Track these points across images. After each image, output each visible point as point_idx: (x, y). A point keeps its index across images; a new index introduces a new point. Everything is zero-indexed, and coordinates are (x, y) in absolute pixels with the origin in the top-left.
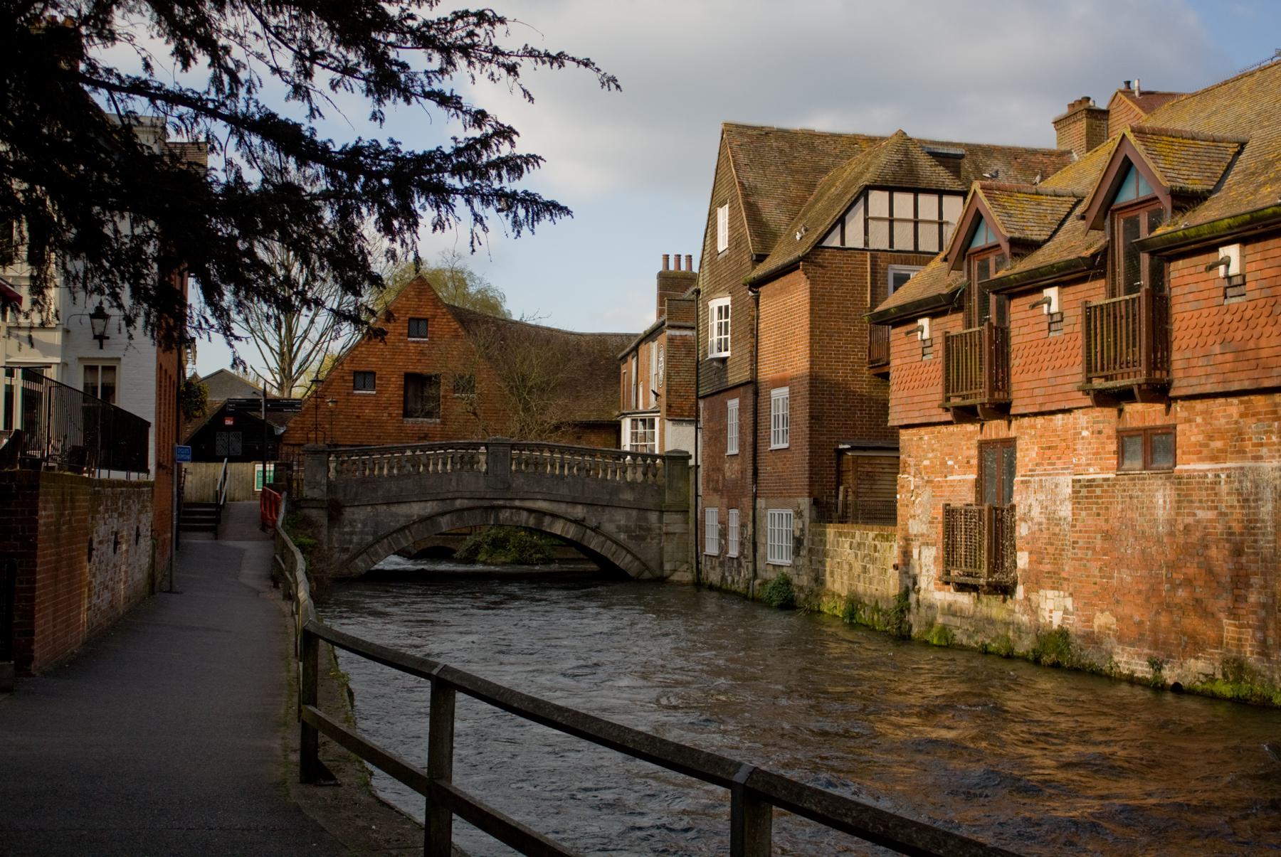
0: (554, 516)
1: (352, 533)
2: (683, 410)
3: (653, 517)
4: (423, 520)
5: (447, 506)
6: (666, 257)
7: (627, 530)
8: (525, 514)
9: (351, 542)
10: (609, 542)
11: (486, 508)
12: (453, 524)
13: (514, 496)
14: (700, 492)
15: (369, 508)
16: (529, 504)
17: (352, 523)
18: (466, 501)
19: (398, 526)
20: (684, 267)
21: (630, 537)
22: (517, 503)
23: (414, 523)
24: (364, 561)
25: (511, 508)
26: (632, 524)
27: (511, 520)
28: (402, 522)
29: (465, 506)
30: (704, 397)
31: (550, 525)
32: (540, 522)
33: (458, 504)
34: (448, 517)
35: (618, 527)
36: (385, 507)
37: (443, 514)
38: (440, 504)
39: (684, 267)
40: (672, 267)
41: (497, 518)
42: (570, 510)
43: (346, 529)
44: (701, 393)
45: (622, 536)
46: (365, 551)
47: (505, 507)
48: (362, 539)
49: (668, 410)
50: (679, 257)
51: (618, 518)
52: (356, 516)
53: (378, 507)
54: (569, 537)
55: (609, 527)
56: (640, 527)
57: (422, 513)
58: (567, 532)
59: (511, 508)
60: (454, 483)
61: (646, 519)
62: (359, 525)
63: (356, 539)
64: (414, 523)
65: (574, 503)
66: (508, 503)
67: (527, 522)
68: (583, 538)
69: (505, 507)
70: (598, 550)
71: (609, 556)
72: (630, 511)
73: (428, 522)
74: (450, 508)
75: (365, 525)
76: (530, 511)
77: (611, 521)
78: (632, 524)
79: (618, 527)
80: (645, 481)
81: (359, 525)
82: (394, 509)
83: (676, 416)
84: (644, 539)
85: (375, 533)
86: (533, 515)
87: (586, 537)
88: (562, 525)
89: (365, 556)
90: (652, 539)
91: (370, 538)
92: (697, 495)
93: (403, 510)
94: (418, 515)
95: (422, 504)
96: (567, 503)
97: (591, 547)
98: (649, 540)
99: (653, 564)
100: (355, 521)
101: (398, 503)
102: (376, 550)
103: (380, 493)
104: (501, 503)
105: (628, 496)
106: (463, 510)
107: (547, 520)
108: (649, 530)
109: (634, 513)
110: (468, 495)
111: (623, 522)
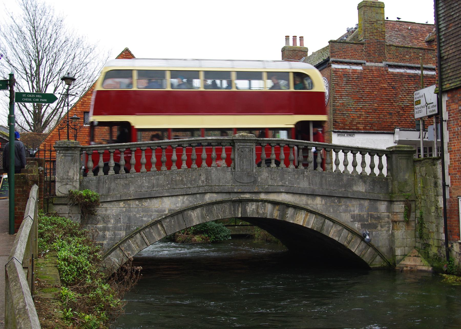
0: (297, 208)
1: (105, 229)
2: (345, 125)
3: (383, 207)
4: (174, 214)
5: (198, 200)
6: (287, 38)
7: (359, 219)
8: (269, 207)
9: (104, 237)
10: (345, 231)
11: (234, 202)
12: (203, 217)
13: (261, 190)
14: (448, 181)
15: (122, 204)
16: (273, 197)
17: (106, 219)
18: (215, 195)
19: (150, 221)
20: (298, 44)
21: (363, 226)
22: (263, 196)
23: (166, 218)
24: (118, 257)
25: (257, 201)
26: (364, 214)
27: (258, 213)
28: (155, 217)
29: (214, 200)
30: (447, 92)
31: (293, 216)
32: (284, 214)
33: (208, 198)
34: (198, 210)
35: (353, 217)
36: (137, 202)
37: (194, 208)
38: (191, 198)
39: (298, 44)
40: (291, 44)
41: (244, 211)
42: (310, 202)
43: (100, 226)
44: (447, 86)
45: (357, 226)
46: (118, 246)
47: (252, 201)
48: (115, 235)
49: (334, 125)
50: (295, 37)
51: (352, 209)
52: (109, 212)
53: (131, 202)
54: (310, 227)
55: (345, 218)
56: (372, 216)
57: (173, 207)
58: (308, 223)
59: (257, 201)
60: (203, 178)
61: (376, 209)
62: (112, 221)
63: (108, 234)
64: (166, 218)
65: (313, 195)
66: (254, 197)
67: (272, 214)
68: (322, 228)
69: (252, 201)
70: (336, 239)
71: (345, 244)
72: (362, 202)
73: (180, 216)
74: (200, 203)
75: (118, 220)
76: (274, 203)
77: (345, 211)
78: (364, 214)
79: (353, 217)
80: (372, 173)
81: (112, 221)
82: (146, 204)
83: (340, 129)
84: (375, 227)
85: (128, 227)
86: (277, 207)
87: (325, 227)
88: (303, 216)
89: (118, 251)
90: (382, 227)
91: (123, 234)
92: (444, 185)
93: (156, 204)
94: (170, 210)
95: (174, 199)
96: (307, 195)
97: (330, 236)
98: (379, 228)
99: (384, 250)
100: (108, 217)
101: (150, 198)
102: (129, 246)
103: (132, 189)
104: (247, 196)
105: (360, 188)
106: (213, 204)
107: (290, 211)
108: (379, 218)
109: (366, 203)
110: (217, 189)
111: (357, 212)
